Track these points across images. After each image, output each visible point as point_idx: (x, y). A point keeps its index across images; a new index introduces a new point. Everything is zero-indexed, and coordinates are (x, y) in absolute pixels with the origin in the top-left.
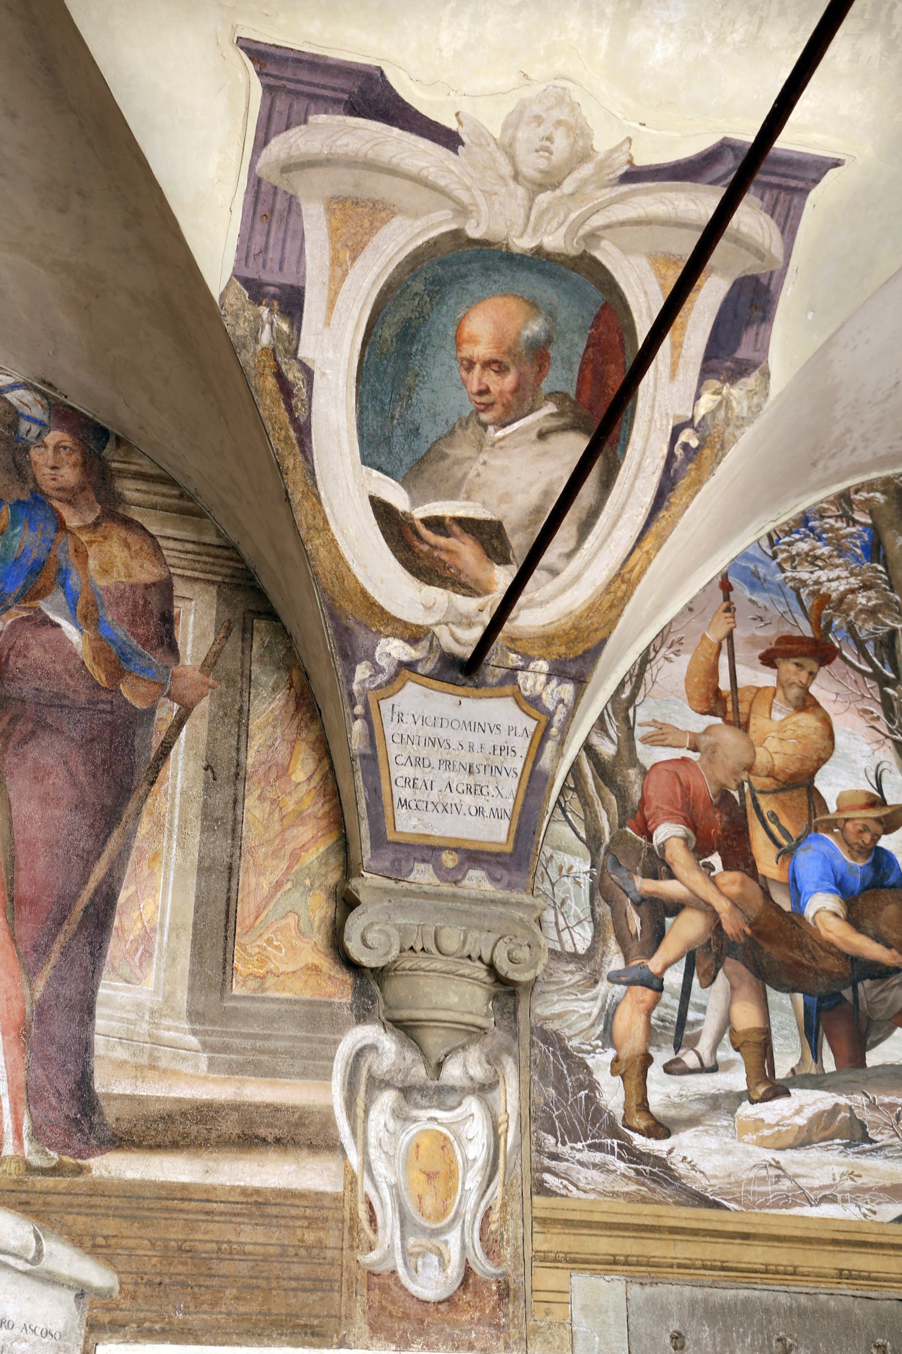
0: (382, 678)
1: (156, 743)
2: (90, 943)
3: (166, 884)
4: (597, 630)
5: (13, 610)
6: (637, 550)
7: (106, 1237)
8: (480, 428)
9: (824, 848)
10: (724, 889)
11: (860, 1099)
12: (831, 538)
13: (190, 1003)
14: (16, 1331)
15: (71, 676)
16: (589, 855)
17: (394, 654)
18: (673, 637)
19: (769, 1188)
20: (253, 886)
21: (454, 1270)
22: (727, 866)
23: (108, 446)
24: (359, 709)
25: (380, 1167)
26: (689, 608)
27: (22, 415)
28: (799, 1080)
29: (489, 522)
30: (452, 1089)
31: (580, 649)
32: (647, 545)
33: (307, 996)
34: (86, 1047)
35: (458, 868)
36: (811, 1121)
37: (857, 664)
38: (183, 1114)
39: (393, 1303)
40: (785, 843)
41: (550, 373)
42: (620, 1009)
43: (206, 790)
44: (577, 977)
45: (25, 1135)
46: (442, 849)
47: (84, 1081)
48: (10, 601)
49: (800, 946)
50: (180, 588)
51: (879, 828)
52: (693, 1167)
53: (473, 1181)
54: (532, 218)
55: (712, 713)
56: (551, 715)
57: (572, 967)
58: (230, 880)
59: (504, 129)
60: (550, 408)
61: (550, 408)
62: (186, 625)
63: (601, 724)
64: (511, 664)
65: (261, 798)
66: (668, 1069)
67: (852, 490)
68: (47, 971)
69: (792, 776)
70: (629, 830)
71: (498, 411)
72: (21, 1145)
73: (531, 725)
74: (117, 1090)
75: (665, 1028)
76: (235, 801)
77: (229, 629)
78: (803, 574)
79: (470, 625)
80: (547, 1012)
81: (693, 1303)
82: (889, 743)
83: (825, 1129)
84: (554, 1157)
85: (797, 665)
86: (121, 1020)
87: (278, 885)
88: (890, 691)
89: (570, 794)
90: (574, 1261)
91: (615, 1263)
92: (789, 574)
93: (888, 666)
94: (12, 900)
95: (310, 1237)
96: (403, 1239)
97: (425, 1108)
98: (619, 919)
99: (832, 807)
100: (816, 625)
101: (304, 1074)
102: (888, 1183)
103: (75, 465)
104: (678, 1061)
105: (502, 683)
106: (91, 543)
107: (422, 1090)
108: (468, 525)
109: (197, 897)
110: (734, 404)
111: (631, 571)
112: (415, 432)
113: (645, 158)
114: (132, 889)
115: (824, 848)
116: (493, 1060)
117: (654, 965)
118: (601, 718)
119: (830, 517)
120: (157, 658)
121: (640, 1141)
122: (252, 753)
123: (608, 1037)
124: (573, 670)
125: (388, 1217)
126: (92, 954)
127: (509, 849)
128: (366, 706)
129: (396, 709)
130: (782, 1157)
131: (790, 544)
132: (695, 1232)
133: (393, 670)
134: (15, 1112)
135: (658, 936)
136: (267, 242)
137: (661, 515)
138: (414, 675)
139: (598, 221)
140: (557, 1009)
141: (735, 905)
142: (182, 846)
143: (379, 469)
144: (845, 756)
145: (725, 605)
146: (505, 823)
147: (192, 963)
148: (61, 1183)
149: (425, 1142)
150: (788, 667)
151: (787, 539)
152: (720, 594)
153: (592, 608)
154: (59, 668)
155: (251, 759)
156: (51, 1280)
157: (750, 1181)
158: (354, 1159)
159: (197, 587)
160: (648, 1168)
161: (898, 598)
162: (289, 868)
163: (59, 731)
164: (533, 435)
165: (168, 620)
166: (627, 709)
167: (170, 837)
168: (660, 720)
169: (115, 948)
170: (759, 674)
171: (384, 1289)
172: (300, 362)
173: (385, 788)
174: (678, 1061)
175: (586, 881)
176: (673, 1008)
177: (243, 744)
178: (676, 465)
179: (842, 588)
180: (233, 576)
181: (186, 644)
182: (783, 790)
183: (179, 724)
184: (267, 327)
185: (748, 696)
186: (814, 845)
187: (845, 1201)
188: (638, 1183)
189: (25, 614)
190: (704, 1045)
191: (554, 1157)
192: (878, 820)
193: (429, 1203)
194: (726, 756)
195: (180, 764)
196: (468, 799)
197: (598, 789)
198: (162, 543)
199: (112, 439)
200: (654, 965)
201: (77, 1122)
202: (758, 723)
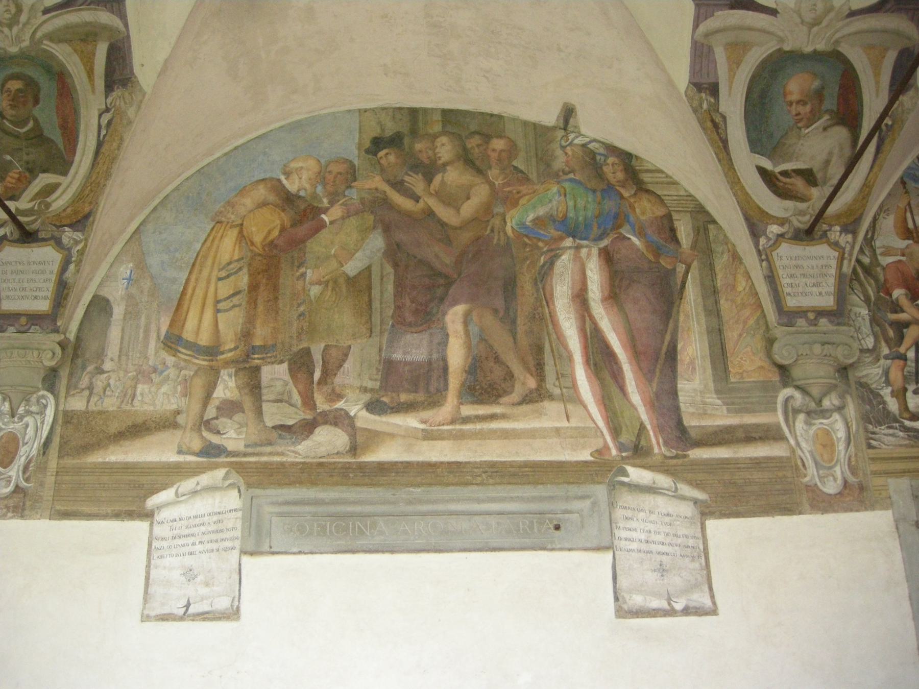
0: (771, 242)
1: (679, 282)
2: (671, 367)
3: (695, 340)
4: (858, 210)
5: (611, 235)
6: (871, 173)
7: (701, 481)
8: (798, 130)
13: (715, 386)
14: (674, 517)
15: (640, 259)
16: (866, 307)
17: (775, 231)
18: (885, 208)
20: (730, 336)
21: (840, 481)
23: (633, 160)
24: (764, 257)
25: (803, 444)
26: (889, 194)
27: (596, 153)
29: (807, 170)
30: (827, 411)
31: (852, 219)
32: (875, 169)
33: (761, 379)
34: (677, 408)
35: (815, 319)
38: (721, 431)
41: (825, 102)
42: (891, 370)
43: (703, 299)
44: (871, 359)
45: (661, 444)
46: (807, 311)
47: (680, 422)
48: (608, 231)
50: (675, 216)
53: (841, 446)
54: (811, 38)
55: (908, 239)
56: (844, 249)
57: (867, 355)
58: (720, 335)
59: (795, 4)
60: (826, 117)
61: (826, 117)
62: (681, 231)
63: (861, 251)
64: (823, 229)
65: (727, 300)
68: (656, 380)
70: (881, 294)
71: (805, 121)
72: (661, 449)
73: (836, 254)
74: (693, 424)
76: (716, 303)
77: (699, 230)
79: (804, 215)
80: (861, 374)
86: (689, 396)
87: (740, 335)
89: (854, 282)
90: (887, 473)
94: (636, 353)
95: (780, 474)
96: (818, 472)
97: (817, 419)
98: (884, 333)
101: (766, 411)
103: (621, 171)
105: (821, 238)
106: (635, 202)
107: (815, 412)
108: (798, 172)
109: (709, 344)
110: (905, 104)
111: (870, 182)
112: (771, 136)
113: (855, 6)
114: (682, 343)
116: (842, 397)
117: (902, 350)
118: (861, 248)
120: (672, 246)
121: (907, 423)
122: (718, 281)
123: (888, 382)
124: (850, 228)
125: (810, 463)
126: (672, 371)
127: (835, 308)
128: (766, 255)
129: (779, 255)
133: (775, 238)
134: (656, 436)
135: (901, 338)
136: (701, 67)
137: (879, 156)
138: (784, 240)
139: (837, 36)
140: (864, 373)
142: (698, 323)
143: (758, 154)
145: (905, 190)
146: (832, 298)
147: (712, 371)
148: (680, 461)
152: (901, 186)
153: (855, 201)
154: (634, 256)
155: (719, 283)
156: (683, 498)
158: (792, 442)
159: (682, 214)
160: (912, 434)
162: (744, 327)
163: (639, 282)
164: (821, 129)
165: (673, 230)
166: (871, 241)
167: (693, 321)
168: (886, 245)
169: (681, 368)
171: (813, 491)
172: (720, 114)
173: (779, 289)
175: (867, 318)
176: (912, 367)
177: (714, 278)
178: (883, 133)
180: (695, 208)
181: (682, 239)
183: (687, 272)
184: (705, 101)
188: (909, 440)
189: (616, 236)
191: (873, 433)
193: (826, 457)
195: (691, 290)
196: (815, 289)
197: (865, 277)
198: (663, 198)
199: (634, 157)
200: (902, 350)
201: (680, 438)
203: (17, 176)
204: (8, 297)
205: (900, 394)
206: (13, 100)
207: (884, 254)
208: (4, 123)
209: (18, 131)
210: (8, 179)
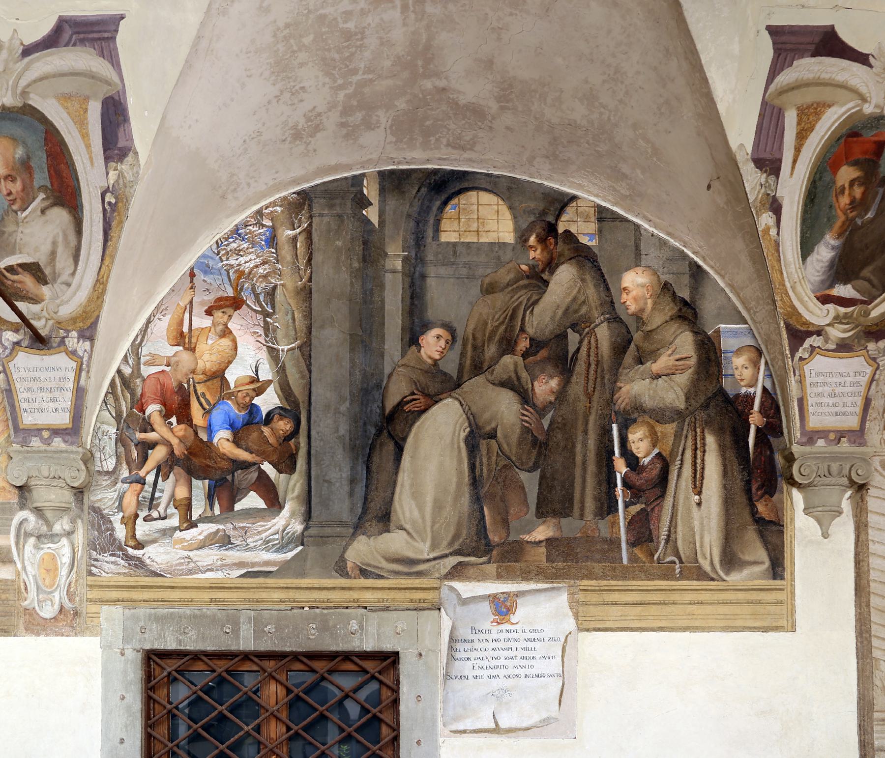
9: (226, 408)
10: (176, 434)
11: (230, 526)
12: (249, 237)
19: (184, 567)
21: (57, 607)
22: (178, 422)
26: (172, 290)
28: (203, 519)
30: (57, 535)
36: (206, 537)
37: (254, 307)
39: (34, 619)
40: (207, 407)
44: (109, 482)
49: (210, 458)
51: (254, 394)
52: (153, 561)
53: (64, 572)
55: (178, 345)
57: (106, 478)
63: (125, 359)
66: (145, 520)
67: (264, 208)
69: (214, 373)
75: (145, 501)
78: (232, 261)
81: (150, 615)
82: (265, 348)
83: (212, 540)
84: (96, 560)
85: (223, 312)
88: (268, 319)
89: (110, 395)
90: (102, 601)
91: (118, 601)
92: (224, 262)
93: (269, 306)
96: (38, 596)
98: (128, 452)
99: (232, 386)
100: (235, 290)
102: (237, 561)
104: (150, 515)
107: (45, 536)
115: (226, 408)
116: (73, 521)
117: (142, 473)
118: (126, 356)
119: (250, 225)
121: (130, 551)
123: (120, 508)
125: (32, 588)
130: (191, 554)
131: (227, 245)
132: (151, 587)
135: (145, 458)
140: (99, 497)
141: (181, 441)
144: (242, 358)
149: (46, 557)
150: (218, 314)
151: (226, 243)
152: (189, 279)
157: (177, 565)
161: (280, 267)
170: (203, 320)
171: (31, 615)
174: (150, 515)
175: (114, 437)
179: (251, 266)
182: (209, 380)
185: (197, 333)
186: (221, 407)
187: (217, 570)
190: (161, 509)
191: (96, 560)
192: (254, 390)
193: (47, 581)
194: (183, 367)
197: (122, 390)
200: (142, 473)
202: (201, 347)
205: (131, 521)
207: (148, 364)
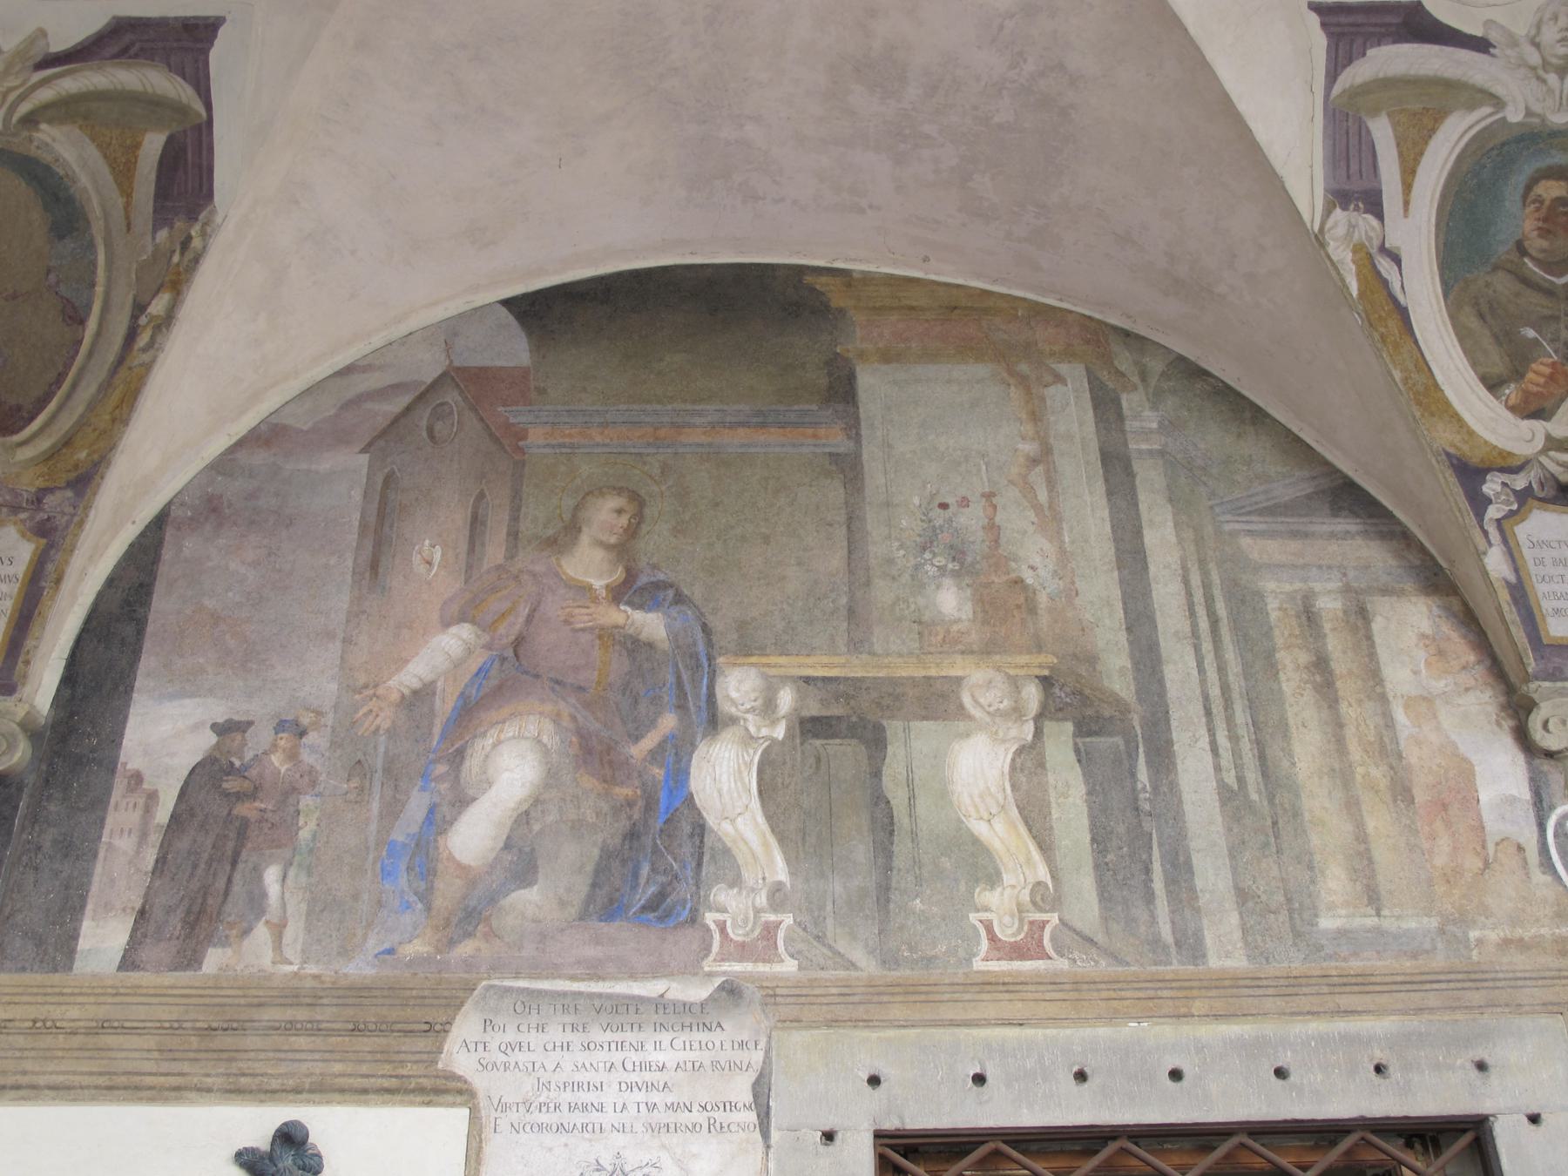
203: (1547, 371)
204: (1557, 611)
206: (1545, 220)
208: (1524, 263)
209: (1552, 283)
210: (1530, 375)
